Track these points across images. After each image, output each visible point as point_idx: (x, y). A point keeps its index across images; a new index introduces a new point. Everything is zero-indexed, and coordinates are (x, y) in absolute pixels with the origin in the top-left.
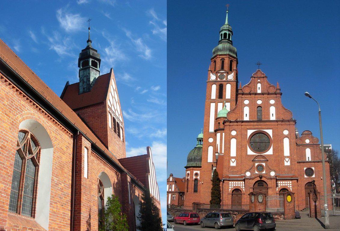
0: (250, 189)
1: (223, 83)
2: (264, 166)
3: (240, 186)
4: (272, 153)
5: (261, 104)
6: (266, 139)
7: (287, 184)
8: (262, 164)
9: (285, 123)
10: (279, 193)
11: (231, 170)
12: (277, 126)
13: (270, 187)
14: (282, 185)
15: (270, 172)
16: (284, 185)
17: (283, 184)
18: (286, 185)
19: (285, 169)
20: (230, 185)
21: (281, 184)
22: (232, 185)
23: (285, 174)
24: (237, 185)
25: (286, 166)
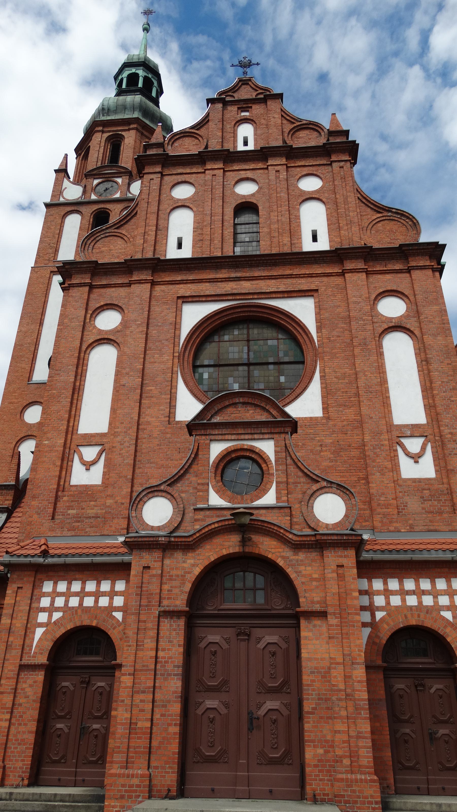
0: (166, 623)
1: (108, 206)
2: (266, 460)
3: (111, 608)
4: (318, 412)
5: (253, 195)
6: (281, 347)
7: (435, 594)
8: (252, 450)
9: (384, 263)
10: (379, 662)
11: (69, 508)
12: (338, 280)
13: (317, 607)
14: (396, 601)
15: (313, 495)
16: (412, 601)
17: (403, 593)
18: (428, 601)
19: (406, 499)
20: (45, 602)
21: (387, 593)
22: (60, 602)
23: (411, 529)
24: (89, 602)
25: (414, 480)
